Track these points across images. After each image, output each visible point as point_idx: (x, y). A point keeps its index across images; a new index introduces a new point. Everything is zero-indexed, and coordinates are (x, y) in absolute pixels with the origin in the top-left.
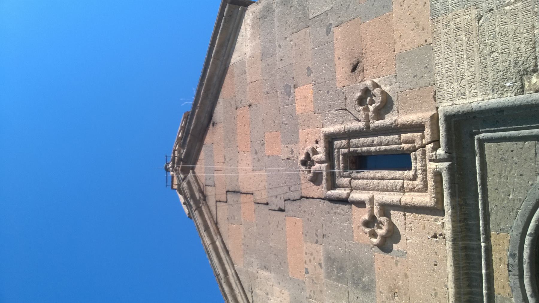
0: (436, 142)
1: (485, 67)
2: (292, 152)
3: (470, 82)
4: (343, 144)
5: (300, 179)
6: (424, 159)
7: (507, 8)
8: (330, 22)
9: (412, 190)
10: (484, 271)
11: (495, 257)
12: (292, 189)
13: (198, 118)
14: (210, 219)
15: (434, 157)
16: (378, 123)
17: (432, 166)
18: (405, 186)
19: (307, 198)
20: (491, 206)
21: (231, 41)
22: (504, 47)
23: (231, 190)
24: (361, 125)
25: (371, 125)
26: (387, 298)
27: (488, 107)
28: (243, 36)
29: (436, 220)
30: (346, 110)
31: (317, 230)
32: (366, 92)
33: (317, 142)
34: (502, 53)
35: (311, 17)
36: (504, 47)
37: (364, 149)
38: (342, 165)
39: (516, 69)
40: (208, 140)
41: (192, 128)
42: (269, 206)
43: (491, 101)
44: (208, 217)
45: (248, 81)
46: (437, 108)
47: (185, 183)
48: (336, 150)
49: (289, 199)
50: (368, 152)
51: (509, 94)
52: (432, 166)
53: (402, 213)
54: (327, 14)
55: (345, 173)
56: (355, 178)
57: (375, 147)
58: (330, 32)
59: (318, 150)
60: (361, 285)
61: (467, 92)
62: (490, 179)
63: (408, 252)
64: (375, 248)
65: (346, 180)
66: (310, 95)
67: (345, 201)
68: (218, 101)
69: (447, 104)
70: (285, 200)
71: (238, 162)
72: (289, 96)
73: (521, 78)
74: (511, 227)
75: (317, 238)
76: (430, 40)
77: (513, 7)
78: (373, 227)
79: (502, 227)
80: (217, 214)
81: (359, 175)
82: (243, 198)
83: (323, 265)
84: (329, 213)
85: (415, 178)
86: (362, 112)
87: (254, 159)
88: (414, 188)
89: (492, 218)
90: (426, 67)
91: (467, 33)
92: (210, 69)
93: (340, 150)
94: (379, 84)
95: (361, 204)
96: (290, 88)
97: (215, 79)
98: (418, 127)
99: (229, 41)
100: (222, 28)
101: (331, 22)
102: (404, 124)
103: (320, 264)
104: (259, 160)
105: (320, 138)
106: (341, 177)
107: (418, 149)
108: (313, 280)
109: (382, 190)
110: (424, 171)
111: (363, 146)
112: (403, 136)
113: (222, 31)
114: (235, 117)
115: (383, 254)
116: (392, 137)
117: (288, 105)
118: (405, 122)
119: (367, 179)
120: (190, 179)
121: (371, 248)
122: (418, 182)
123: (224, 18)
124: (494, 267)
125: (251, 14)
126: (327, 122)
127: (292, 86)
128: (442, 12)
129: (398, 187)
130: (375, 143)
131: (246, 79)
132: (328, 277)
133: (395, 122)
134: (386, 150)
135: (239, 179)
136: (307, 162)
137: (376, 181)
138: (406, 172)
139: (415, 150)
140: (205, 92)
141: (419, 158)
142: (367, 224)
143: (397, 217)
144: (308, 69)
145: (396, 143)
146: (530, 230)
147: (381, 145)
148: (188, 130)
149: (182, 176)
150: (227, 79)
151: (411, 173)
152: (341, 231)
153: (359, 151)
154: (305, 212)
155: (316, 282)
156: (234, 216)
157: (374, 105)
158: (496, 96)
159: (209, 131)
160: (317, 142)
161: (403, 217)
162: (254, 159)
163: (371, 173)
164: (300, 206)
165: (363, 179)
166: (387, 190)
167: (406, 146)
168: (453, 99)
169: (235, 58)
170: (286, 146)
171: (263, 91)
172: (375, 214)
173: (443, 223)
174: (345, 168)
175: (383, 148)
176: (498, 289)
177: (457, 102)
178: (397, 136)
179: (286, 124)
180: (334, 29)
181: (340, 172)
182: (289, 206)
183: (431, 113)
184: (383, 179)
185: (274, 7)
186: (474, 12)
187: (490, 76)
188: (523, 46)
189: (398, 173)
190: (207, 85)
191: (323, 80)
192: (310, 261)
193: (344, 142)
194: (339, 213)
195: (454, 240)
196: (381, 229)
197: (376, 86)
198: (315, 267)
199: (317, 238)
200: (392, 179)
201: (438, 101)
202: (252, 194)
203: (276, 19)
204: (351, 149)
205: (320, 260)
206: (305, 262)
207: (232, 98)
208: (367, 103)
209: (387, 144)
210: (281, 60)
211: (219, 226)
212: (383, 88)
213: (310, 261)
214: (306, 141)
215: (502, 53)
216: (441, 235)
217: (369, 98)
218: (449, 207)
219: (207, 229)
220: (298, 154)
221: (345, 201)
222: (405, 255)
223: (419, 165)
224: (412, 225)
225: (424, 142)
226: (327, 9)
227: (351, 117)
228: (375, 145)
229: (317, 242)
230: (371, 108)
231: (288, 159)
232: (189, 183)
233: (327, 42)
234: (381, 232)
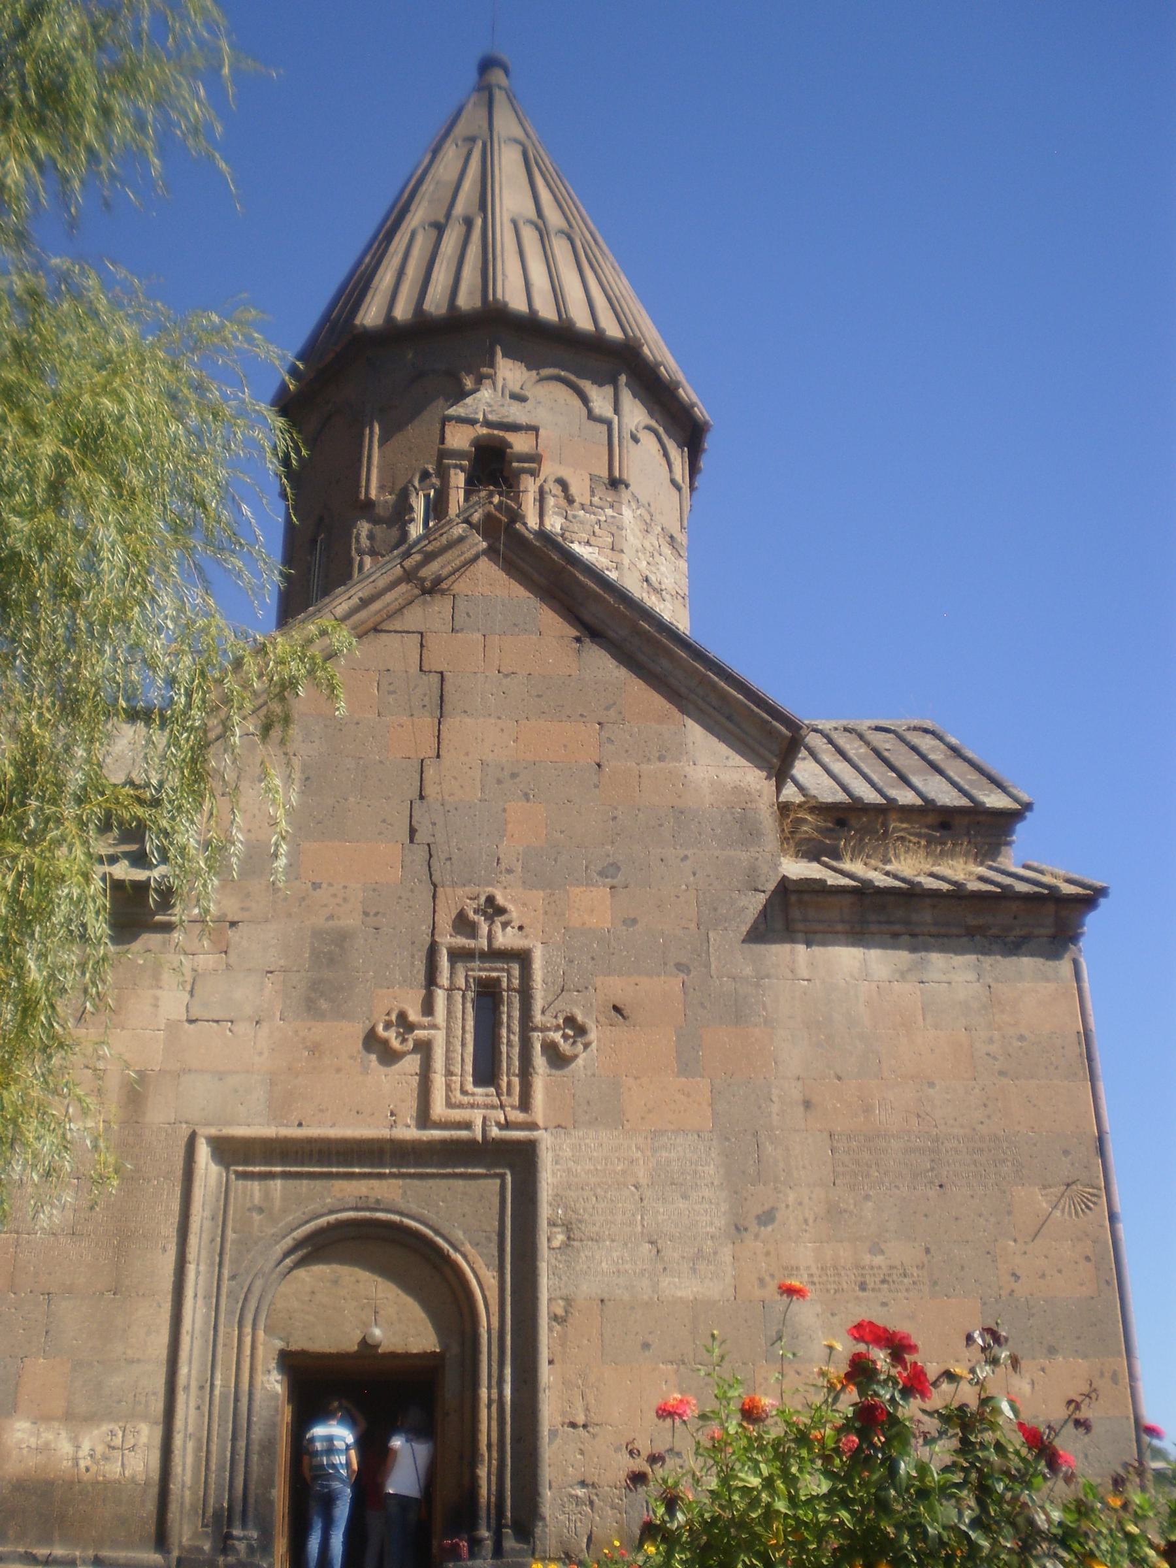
0: (507, 1125)
1: (582, 1189)
2: (509, 871)
3: (569, 1170)
4: (514, 981)
5: (464, 885)
6: (487, 1106)
7: (639, 1217)
8: (692, 968)
9: (448, 1087)
10: (357, 1170)
11: (375, 1183)
12: (448, 863)
13: (597, 598)
14: (385, 608)
15: (488, 1123)
16: (538, 1047)
17: (477, 1117)
18: (454, 1078)
19: (434, 897)
20: (431, 1182)
21: (728, 724)
22: (600, 1211)
23: (448, 687)
24: (538, 1018)
25: (536, 1034)
26: (304, 1039)
27: (539, 1191)
28: (727, 758)
29: (412, 1117)
30: (562, 991)
31: (384, 915)
32: (581, 1031)
33: (521, 928)
34: (594, 1208)
35: (711, 934)
36: (600, 1211)
37: (505, 1017)
38: (483, 974)
39: (574, 1221)
40: (550, 620)
41: (578, 574)
42: (418, 801)
43: (545, 1194)
44: (388, 605)
45: (644, 767)
46: (546, 1129)
47: (460, 531)
48: (506, 967)
49: (431, 856)
50: (500, 1024)
51: (550, 1212)
52: (477, 1117)
53: (418, 1071)
54: (706, 967)
55: (471, 980)
56: (464, 997)
57: (505, 1035)
58: (679, 970)
59: (509, 928)
60: (313, 995)
61: (558, 1167)
62: (461, 1182)
63: (370, 1077)
64: (369, 1025)
65: (461, 982)
66: (592, 921)
67: (431, 980)
68: (622, 667)
69: (549, 1142)
70: (429, 845)
71: (499, 718)
72: (602, 874)
73: (563, 1225)
74: (408, 1202)
75: (372, 914)
76: (628, 1126)
77: (639, 1223)
78: (398, 1026)
79: (409, 1193)
80: (396, 632)
81: (469, 1005)
82: (427, 722)
83: (331, 922)
84: (413, 943)
85: (464, 1092)
86: (554, 1022)
87: (503, 769)
88: (451, 1091)
89: (416, 1182)
90: (597, 1119)
91: (624, 1172)
92: (685, 659)
93: (505, 974)
94: (589, 1049)
95: (428, 1008)
96: (613, 877)
97: (665, 663)
98: (525, 1104)
99: (729, 718)
100: (753, 711)
101: (693, 973)
102: (531, 1086)
103: (331, 917)
104: (499, 782)
105: (526, 937)
106: (466, 972)
107: (500, 1100)
108: (304, 899)
109: (448, 1043)
110: (472, 1106)
111: (509, 1017)
112: (516, 1081)
113: (749, 708)
114: (584, 719)
115: (361, 1036)
116: (517, 1064)
117: (586, 867)
118: (534, 1088)
119: (463, 1019)
120: (470, 541)
121: (368, 1019)
122: (458, 1097)
123: (770, 719)
124: (362, 1182)
125: (758, 787)
126: (548, 952)
127: (615, 882)
128: (656, 1144)
129: (452, 1068)
130: (512, 1037)
131: (649, 760)
132: (317, 934)
133: (536, 1073)
134: (501, 1053)
135: (467, 720)
136: (493, 909)
137: (460, 1032)
138: (471, 1079)
139: (498, 1095)
140: (647, 632)
141: (488, 1100)
142: (402, 1016)
143: (412, 1063)
144: (634, 921)
145: (508, 1069)
146: (406, 1221)
147: (507, 1045)
148: (573, 565)
149: (476, 517)
150: (657, 701)
151: (470, 1087)
152: (387, 966)
153: (502, 1008)
154: (412, 891)
155: (303, 904)
156: (394, 692)
157: (562, 1041)
158: (550, 1198)
159: (566, 625)
160: (521, 928)
161: (413, 1072)
162: (503, 769)
163: (470, 1024)
164: (420, 881)
165: (464, 1012)
166: (447, 1051)
167: (504, 1085)
168: (554, 1150)
169: (695, 732)
170: (520, 857)
171: (620, 808)
172: (416, 1032)
173: (409, 1126)
174: (480, 982)
175: (504, 1048)
176: (339, 1184)
177: (550, 1154)
178: (517, 1071)
179: (556, 860)
180: (682, 976)
181: (473, 970)
182: (421, 853)
183: (541, 1123)
184: (463, 1045)
185: (752, 849)
186: (644, 1181)
187: (572, 1194)
188: (596, 1229)
189: (469, 1068)
190: (658, 642)
191: (612, 950)
192: (334, 896)
193: (516, 982)
194: (413, 964)
195: (392, 1141)
196: (396, 1038)
197: (586, 1046)
198: (326, 906)
199: (372, 914)
200: (463, 1060)
201: (554, 1131)
202: (438, 756)
203: (732, 853)
204: (505, 994)
205: (339, 919)
206: (330, 885)
207: (620, 713)
208: (567, 1031)
209: (508, 1057)
210: (662, 860)
211: (372, 635)
212: (583, 1056)
213: (334, 896)
214: (524, 905)
215: (594, 1208)
216: (395, 1121)
217: (570, 1033)
218: (430, 1138)
219: (365, 603)
220: (505, 884)
221: (431, 980)
222: (365, 1070)
223: (480, 1100)
224: (405, 1084)
225: (508, 1109)
226: (713, 967)
227: (549, 999)
228: (508, 1037)
229: (366, 914)
230: (557, 1037)
231: (498, 859)
232: (461, 539)
233: (665, 964)
234: (391, 1036)
